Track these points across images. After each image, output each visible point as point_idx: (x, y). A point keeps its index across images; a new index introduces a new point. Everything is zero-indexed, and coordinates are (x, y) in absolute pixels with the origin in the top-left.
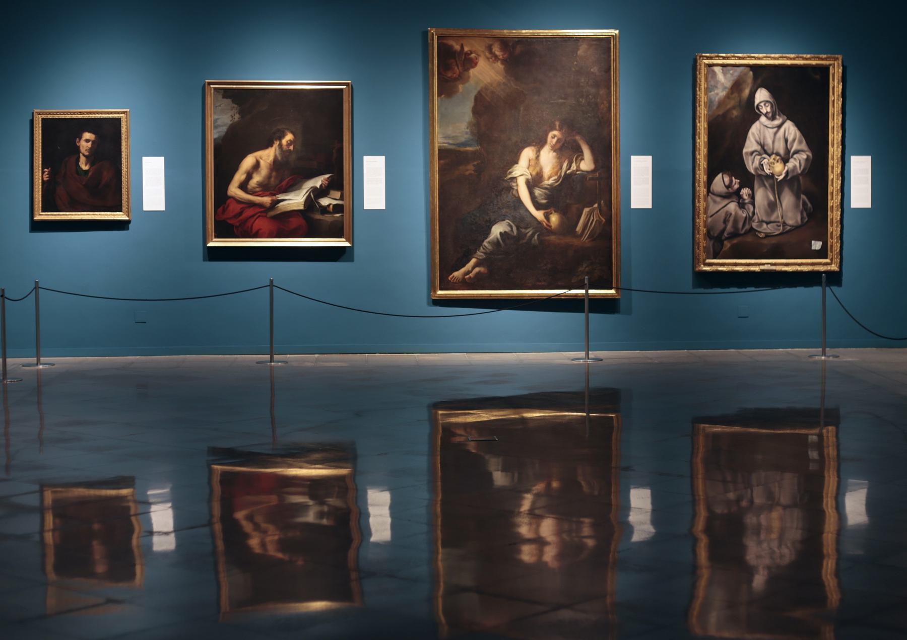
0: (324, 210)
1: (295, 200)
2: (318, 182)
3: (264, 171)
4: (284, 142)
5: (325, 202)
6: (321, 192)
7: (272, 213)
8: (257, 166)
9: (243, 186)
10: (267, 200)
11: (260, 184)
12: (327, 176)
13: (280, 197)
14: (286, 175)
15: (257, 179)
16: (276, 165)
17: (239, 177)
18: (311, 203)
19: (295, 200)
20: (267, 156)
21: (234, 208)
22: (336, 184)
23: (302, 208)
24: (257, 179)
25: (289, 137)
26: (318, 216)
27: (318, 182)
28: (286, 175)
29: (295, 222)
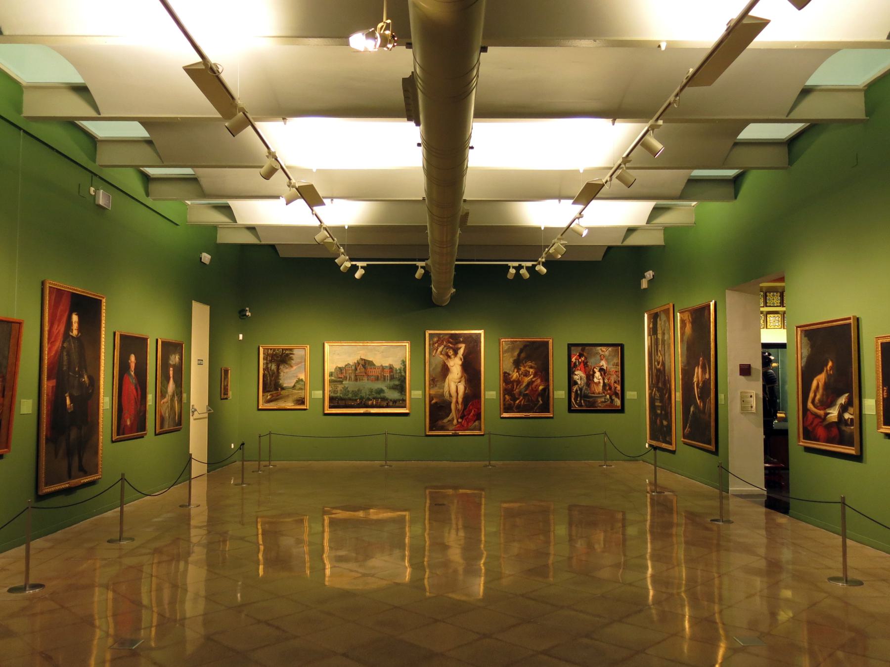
1: (834, 413)
2: (842, 400)
3: (821, 390)
5: (847, 416)
16: (826, 386)
18: (840, 415)
21: (810, 417)
24: (818, 397)
25: (830, 364)
27: (842, 400)
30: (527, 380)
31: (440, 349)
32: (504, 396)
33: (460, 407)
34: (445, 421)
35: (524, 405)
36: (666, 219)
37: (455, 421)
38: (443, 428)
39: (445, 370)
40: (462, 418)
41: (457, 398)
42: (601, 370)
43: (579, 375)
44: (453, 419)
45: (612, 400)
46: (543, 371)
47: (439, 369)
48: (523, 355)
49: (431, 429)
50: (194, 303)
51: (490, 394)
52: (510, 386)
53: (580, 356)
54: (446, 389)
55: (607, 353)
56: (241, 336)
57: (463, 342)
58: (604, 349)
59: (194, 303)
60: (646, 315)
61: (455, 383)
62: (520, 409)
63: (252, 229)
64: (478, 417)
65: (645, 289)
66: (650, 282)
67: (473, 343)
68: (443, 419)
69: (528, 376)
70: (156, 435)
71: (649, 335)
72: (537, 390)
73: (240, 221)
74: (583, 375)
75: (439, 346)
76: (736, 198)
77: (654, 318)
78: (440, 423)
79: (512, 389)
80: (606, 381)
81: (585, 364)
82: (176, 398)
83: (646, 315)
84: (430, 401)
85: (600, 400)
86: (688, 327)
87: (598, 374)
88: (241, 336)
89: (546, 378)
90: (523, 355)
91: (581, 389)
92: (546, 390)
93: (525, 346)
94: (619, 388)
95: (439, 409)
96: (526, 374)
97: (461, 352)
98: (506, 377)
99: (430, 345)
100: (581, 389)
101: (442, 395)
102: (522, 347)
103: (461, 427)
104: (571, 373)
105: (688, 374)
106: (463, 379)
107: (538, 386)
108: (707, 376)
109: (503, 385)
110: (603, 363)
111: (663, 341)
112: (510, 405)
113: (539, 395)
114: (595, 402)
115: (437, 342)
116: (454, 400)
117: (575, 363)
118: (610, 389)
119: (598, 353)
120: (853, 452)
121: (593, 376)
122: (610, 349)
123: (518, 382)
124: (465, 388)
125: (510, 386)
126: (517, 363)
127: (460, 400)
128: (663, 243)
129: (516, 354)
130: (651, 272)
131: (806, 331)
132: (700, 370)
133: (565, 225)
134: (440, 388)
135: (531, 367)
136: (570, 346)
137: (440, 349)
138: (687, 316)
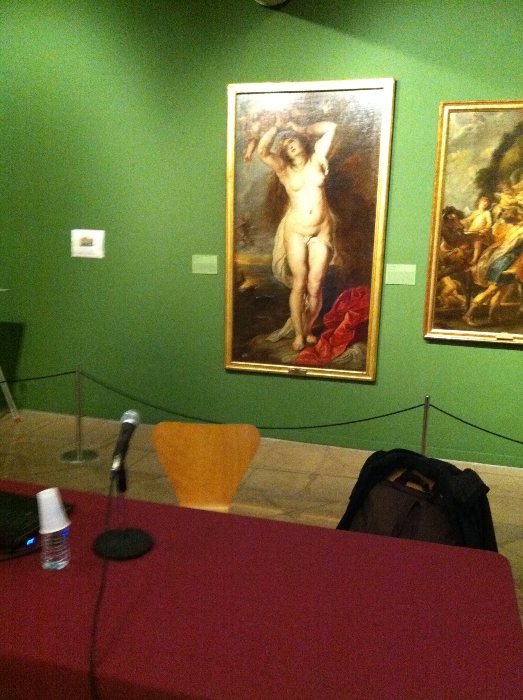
32: (439, 279)
33: (312, 302)
34: (274, 337)
35: (499, 309)
37: (298, 341)
38: (265, 356)
39: (278, 201)
40: (316, 332)
41: (306, 279)
44: (293, 335)
47: (261, 198)
48: (511, 156)
49: (237, 356)
51: (402, 272)
52: (459, 251)
54: (278, 254)
61: (303, 240)
62: (485, 318)
64: (360, 332)
68: (269, 331)
78: (260, 342)
84: (237, 284)
90: (511, 156)
95: (259, 304)
98: (451, 223)
101: (267, 270)
103: (314, 357)
106: (325, 230)
112: (456, 305)
116: (297, 284)
123: (488, 240)
124: (330, 252)
125: (459, 251)
127: (314, 285)
129: (488, 151)
134: (262, 250)
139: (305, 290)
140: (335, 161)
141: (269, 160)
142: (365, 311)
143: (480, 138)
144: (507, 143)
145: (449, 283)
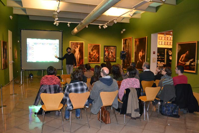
0: (192, 65)
1: (188, 63)
2: (191, 60)
3: (184, 58)
4: (187, 53)
5: (192, 64)
6: (192, 62)
7: (185, 65)
8: (183, 57)
9: (181, 60)
10: (184, 63)
11: (183, 60)
12: (193, 59)
13: (186, 63)
14: (187, 59)
15: (183, 59)
16: (186, 57)
17: (180, 59)
18: (190, 64)
19: (188, 63)
20: (184, 55)
22: (194, 61)
23: (189, 65)
24: (183, 59)
25: (188, 52)
26: (191, 67)
27: (191, 60)
28: (187, 59)
29: (188, 67)
30: (94, 54)
31: (73, 46)
33: (78, 61)
35: (94, 60)
36: (135, 16)
40: (79, 63)
42: (111, 52)
43: (106, 53)
45: (113, 59)
46: (98, 52)
50: (9, 30)
52: (90, 56)
53: (107, 49)
55: (113, 48)
56: (18, 41)
57: (79, 45)
58: (112, 47)
59: (9, 30)
60: (123, 40)
63: (24, 10)
65: (122, 33)
66: (124, 32)
67: (82, 44)
69: (94, 53)
70: (2, 70)
71: (123, 44)
72: (97, 57)
73: (24, 7)
74: (107, 53)
75: (73, 45)
76: (156, 12)
77: (125, 40)
79: (91, 57)
80: (112, 55)
81: (108, 51)
82: (6, 59)
83: (123, 40)
85: (111, 59)
86: (138, 43)
87: (110, 53)
88: (18, 41)
89: (99, 54)
90: (94, 48)
91: (107, 57)
92: (99, 56)
93: (94, 46)
94: (115, 56)
96: (94, 53)
97: (79, 47)
99: (71, 45)
100: (107, 57)
102: (93, 46)
104: (105, 53)
105: (137, 54)
106: (79, 54)
107: (97, 56)
108: (144, 54)
109: (89, 55)
110: (112, 51)
111: (128, 46)
113: (97, 58)
114: (110, 60)
115: (73, 44)
116: (77, 59)
117: (105, 50)
118: (113, 57)
119: (111, 48)
120: (195, 72)
121: (109, 53)
122: (113, 47)
123: (92, 55)
125: (90, 56)
126: (92, 50)
127: (78, 59)
128: (129, 22)
130: (125, 29)
131: (179, 44)
132: (141, 52)
133: (119, 16)
135: (95, 51)
136: (105, 46)
137: (73, 46)
138: (137, 40)
139: (78, 60)
140: (80, 48)
141: (74, 48)
142: (83, 61)
143: (91, 47)
144: (93, 47)
145: (90, 58)
